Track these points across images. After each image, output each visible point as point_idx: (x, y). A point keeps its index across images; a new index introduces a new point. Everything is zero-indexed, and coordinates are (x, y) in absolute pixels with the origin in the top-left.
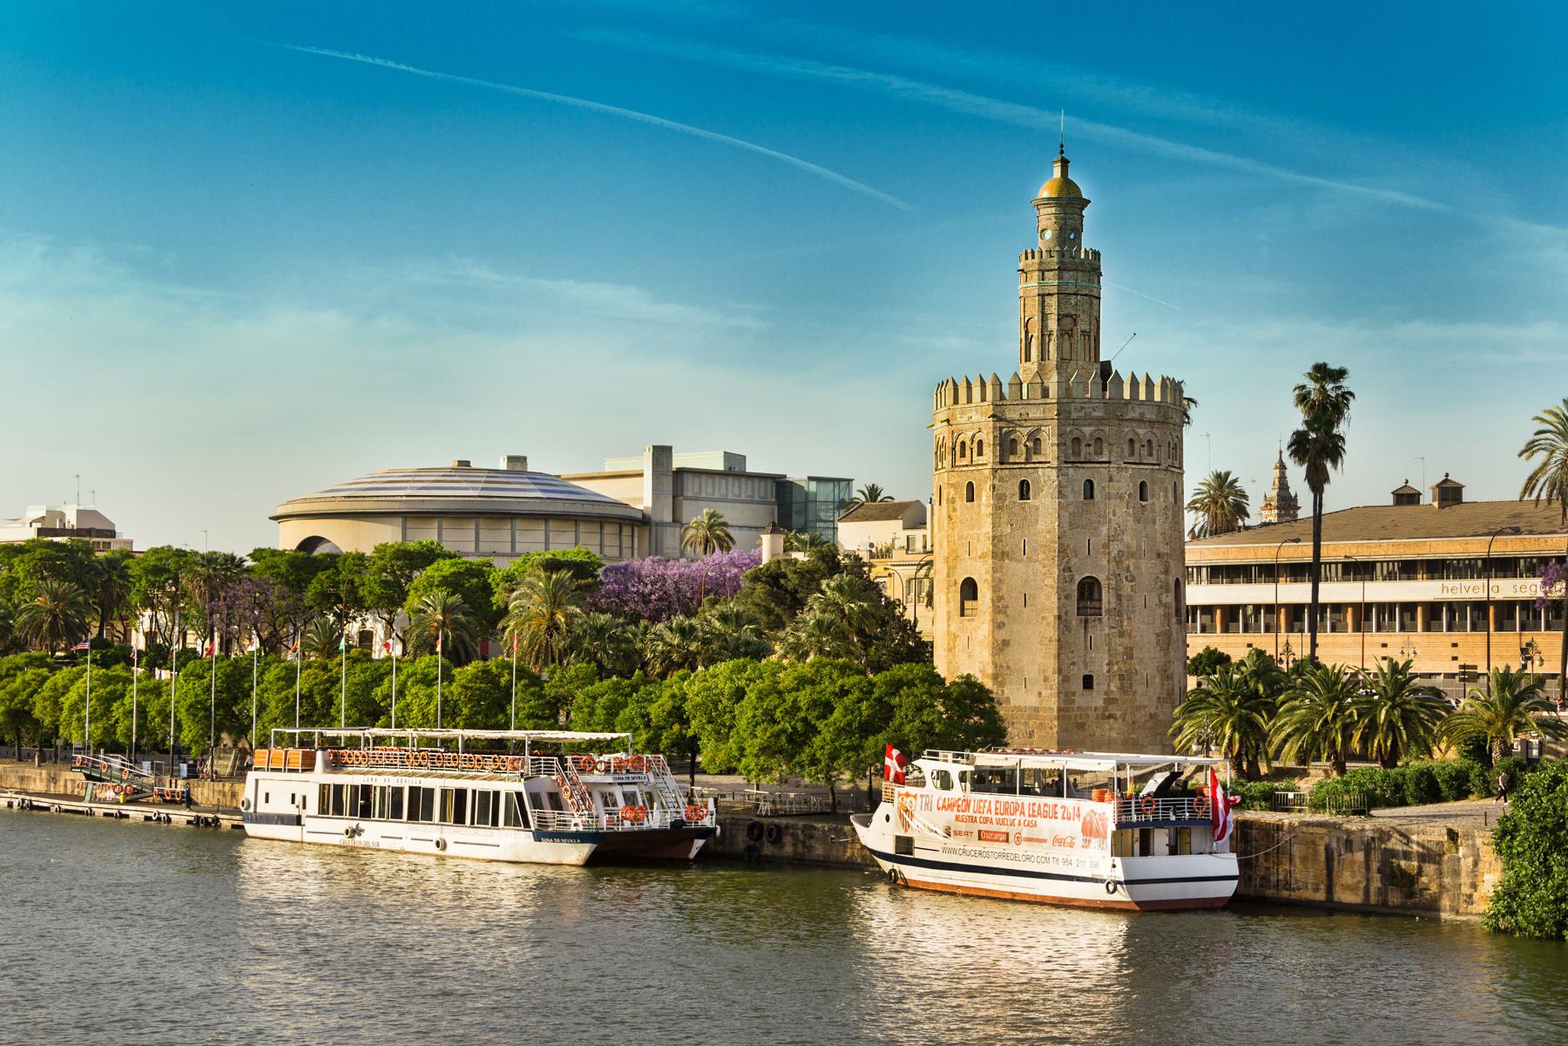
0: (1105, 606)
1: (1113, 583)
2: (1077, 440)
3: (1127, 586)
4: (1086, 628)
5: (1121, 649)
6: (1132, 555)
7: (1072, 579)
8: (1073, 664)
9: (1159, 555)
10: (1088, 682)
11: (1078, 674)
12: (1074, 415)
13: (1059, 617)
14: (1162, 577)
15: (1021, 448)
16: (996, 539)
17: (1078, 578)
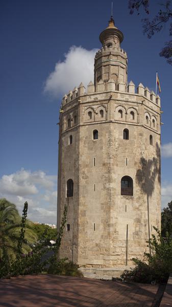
6: (87, 166)
7: (64, 181)
9: (104, 165)
14: (107, 175)
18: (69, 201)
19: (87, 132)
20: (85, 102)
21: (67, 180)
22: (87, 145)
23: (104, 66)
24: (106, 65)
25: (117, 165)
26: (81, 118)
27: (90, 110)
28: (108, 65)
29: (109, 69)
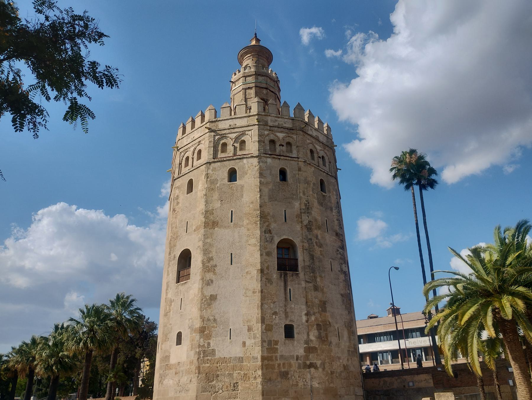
0: (300, 264)
1: (306, 245)
2: (272, 142)
3: (317, 250)
5: (317, 301)
6: (319, 228)
7: (272, 239)
8: (275, 313)
10: (289, 331)
11: (280, 322)
12: (270, 124)
16: (208, 213)
17: (277, 240)
18: (289, 279)
24: (272, 92)
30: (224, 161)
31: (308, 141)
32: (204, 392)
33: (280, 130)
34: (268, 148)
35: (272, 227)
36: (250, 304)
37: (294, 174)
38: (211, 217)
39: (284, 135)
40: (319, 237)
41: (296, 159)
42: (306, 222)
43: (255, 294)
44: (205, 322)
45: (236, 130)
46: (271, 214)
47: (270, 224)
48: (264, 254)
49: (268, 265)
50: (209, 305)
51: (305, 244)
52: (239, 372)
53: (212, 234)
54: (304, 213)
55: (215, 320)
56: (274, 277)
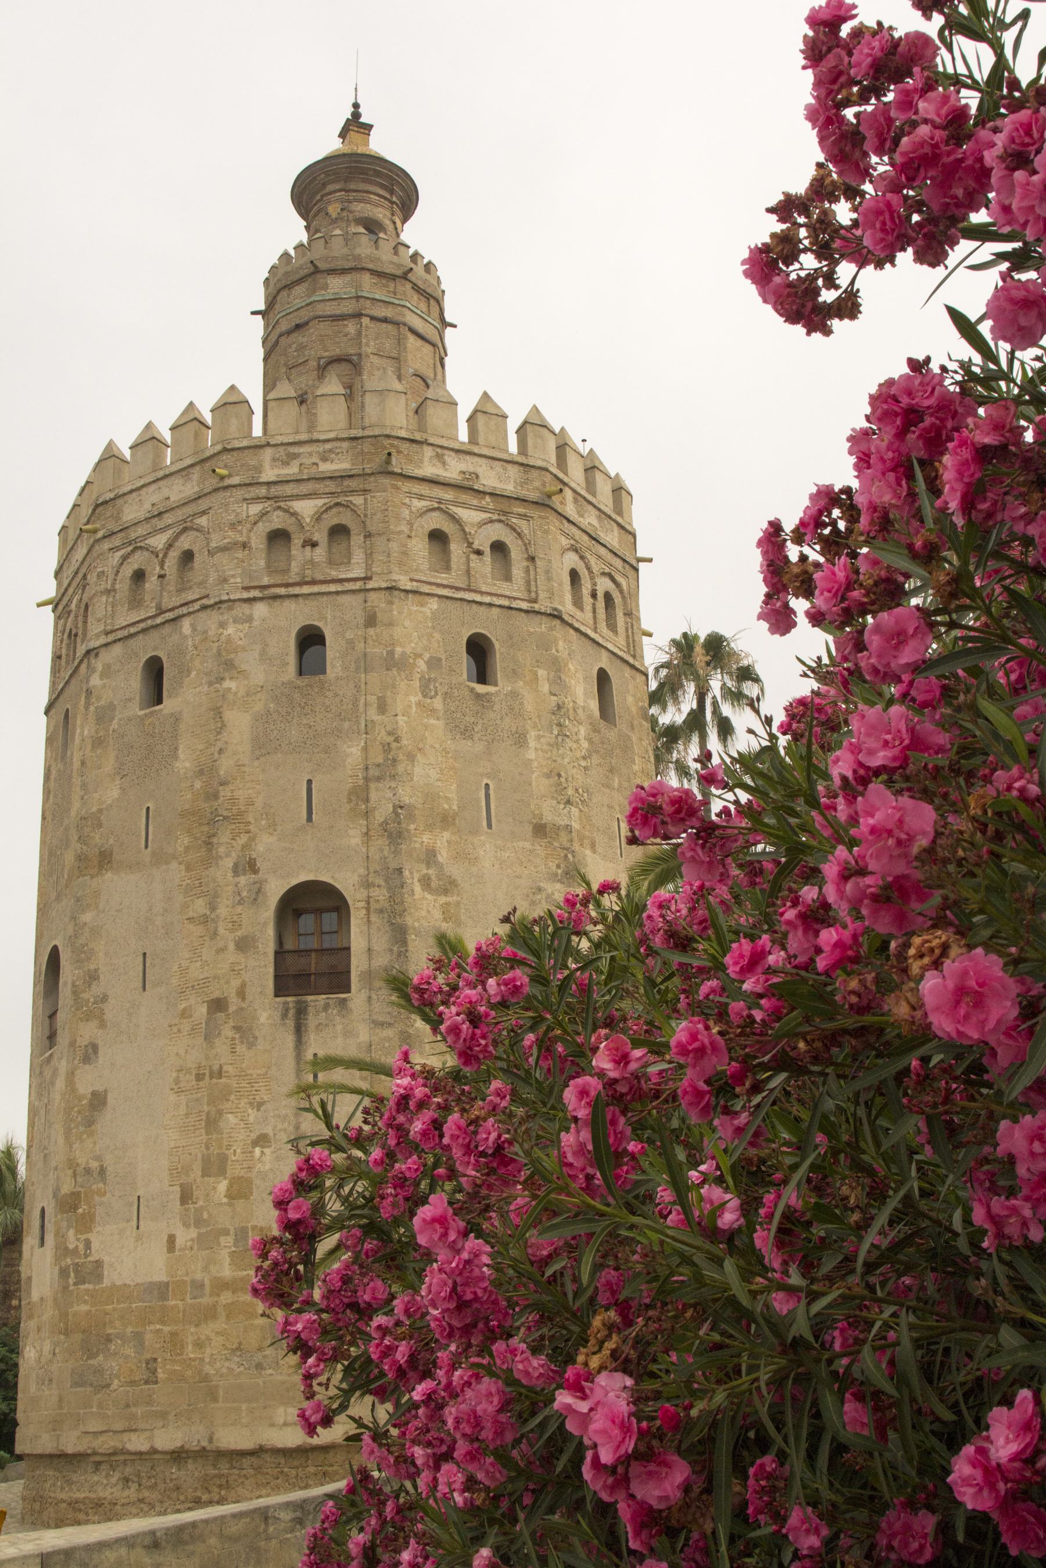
0: (358, 964)
1: (381, 895)
2: (278, 537)
4: (299, 1030)
6: (446, 820)
7: (258, 892)
8: (262, 1140)
9: (540, 830)
12: (269, 474)
13: (218, 1005)
15: (151, 583)
18: (312, 1021)
19: (437, 636)
20: (419, 473)
21: (276, 889)
22: (438, 703)
23: (373, 318)
24: (385, 320)
25: (593, 846)
26: (394, 546)
27: (436, 521)
28: (397, 324)
29: (400, 341)
30: (131, 636)
31: (418, 504)
32: (76, 1384)
33: (304, 488)
34: (262, 563)
35: (261, 848)
36: (187, 1115)
37: (351, 643)
38: (97, 838)
39: (320, 502)
40: (443, 857)
41: (358, 585)
42: (383, 811)
43: (201, 1084)
44: (80, 1180)
45: (169, 519)
46: (259, 802)
47: (253, 839)
48: (231, 946)
49: (243, 985)
50: (90, 1123)
51: (375, 893)
52: (158, 1327)
53: (97, 894)
54: (378, 779)
55: (102, 1171)
56: (263, 1020)
